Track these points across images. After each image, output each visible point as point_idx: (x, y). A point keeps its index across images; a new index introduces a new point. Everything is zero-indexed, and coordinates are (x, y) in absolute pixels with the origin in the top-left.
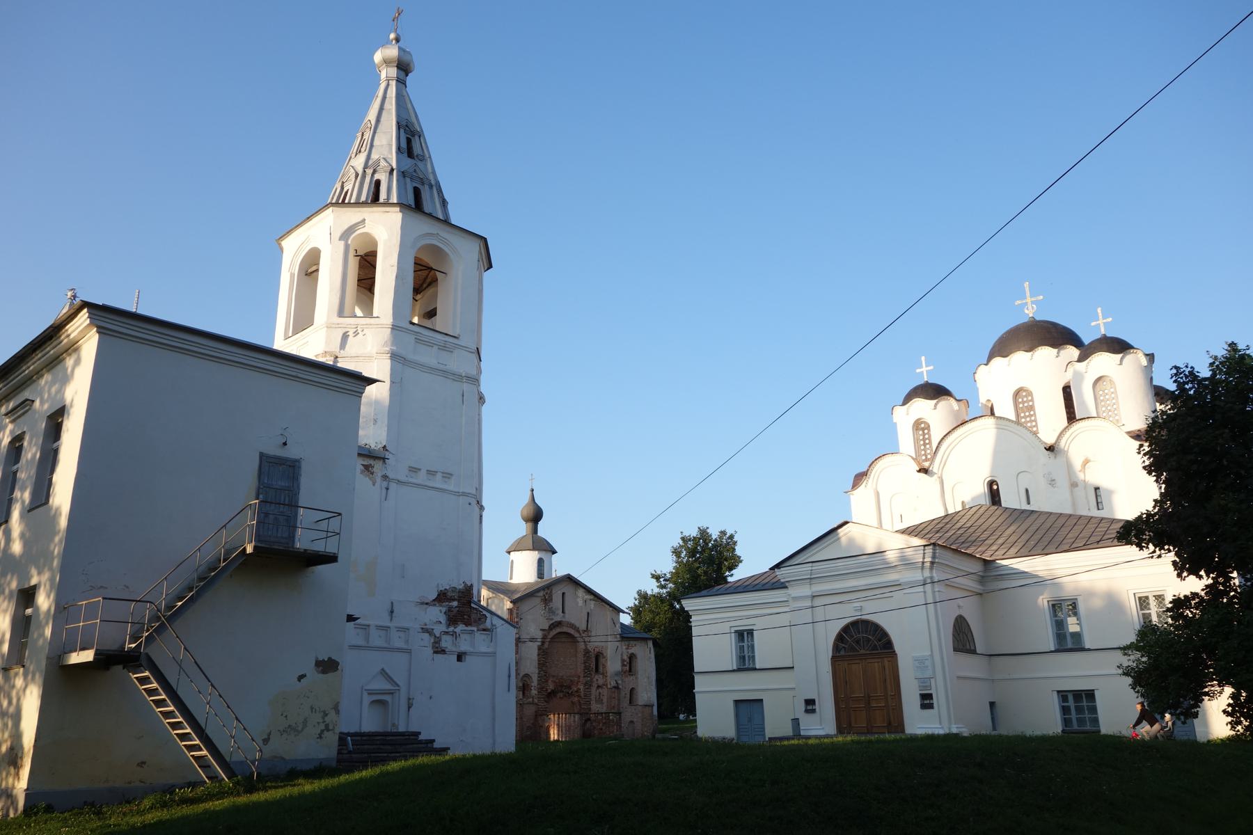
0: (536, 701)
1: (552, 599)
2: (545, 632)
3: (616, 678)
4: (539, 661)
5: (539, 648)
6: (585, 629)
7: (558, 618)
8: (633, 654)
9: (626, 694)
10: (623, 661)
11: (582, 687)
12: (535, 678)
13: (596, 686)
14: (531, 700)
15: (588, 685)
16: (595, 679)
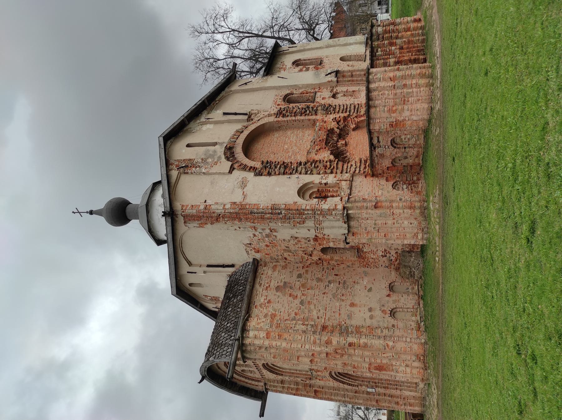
0: (347, 176)
1: (190, 160)
2: (236, 166)
3: (323, 75)
4: (279, 174)
5: (259, 174)
6: (246, 117)
7: (220, 150)
8: (293, 63)
9: (349, 66)
10: (301, 70)
11: (332, 116)
12: (306, 179)
13: (332, 99)
14: (344, 183)
15: (328, 109)
16: (323, 102)
